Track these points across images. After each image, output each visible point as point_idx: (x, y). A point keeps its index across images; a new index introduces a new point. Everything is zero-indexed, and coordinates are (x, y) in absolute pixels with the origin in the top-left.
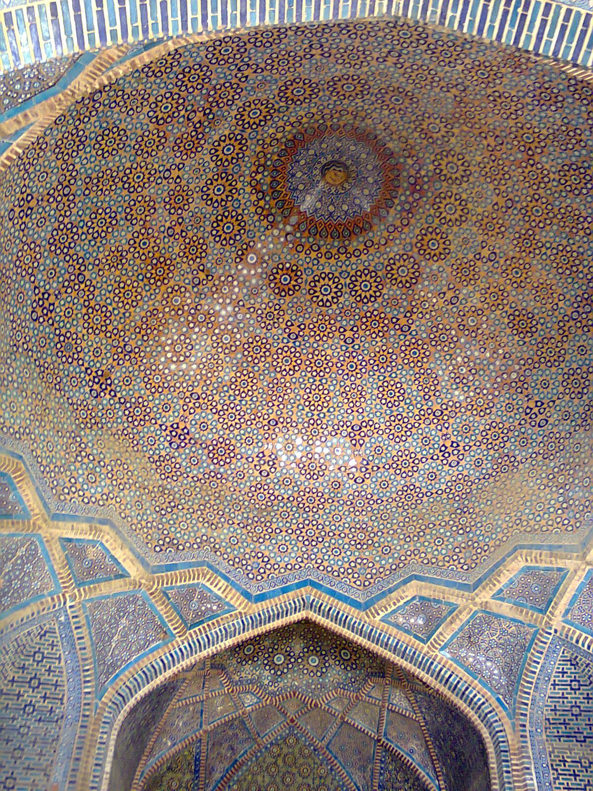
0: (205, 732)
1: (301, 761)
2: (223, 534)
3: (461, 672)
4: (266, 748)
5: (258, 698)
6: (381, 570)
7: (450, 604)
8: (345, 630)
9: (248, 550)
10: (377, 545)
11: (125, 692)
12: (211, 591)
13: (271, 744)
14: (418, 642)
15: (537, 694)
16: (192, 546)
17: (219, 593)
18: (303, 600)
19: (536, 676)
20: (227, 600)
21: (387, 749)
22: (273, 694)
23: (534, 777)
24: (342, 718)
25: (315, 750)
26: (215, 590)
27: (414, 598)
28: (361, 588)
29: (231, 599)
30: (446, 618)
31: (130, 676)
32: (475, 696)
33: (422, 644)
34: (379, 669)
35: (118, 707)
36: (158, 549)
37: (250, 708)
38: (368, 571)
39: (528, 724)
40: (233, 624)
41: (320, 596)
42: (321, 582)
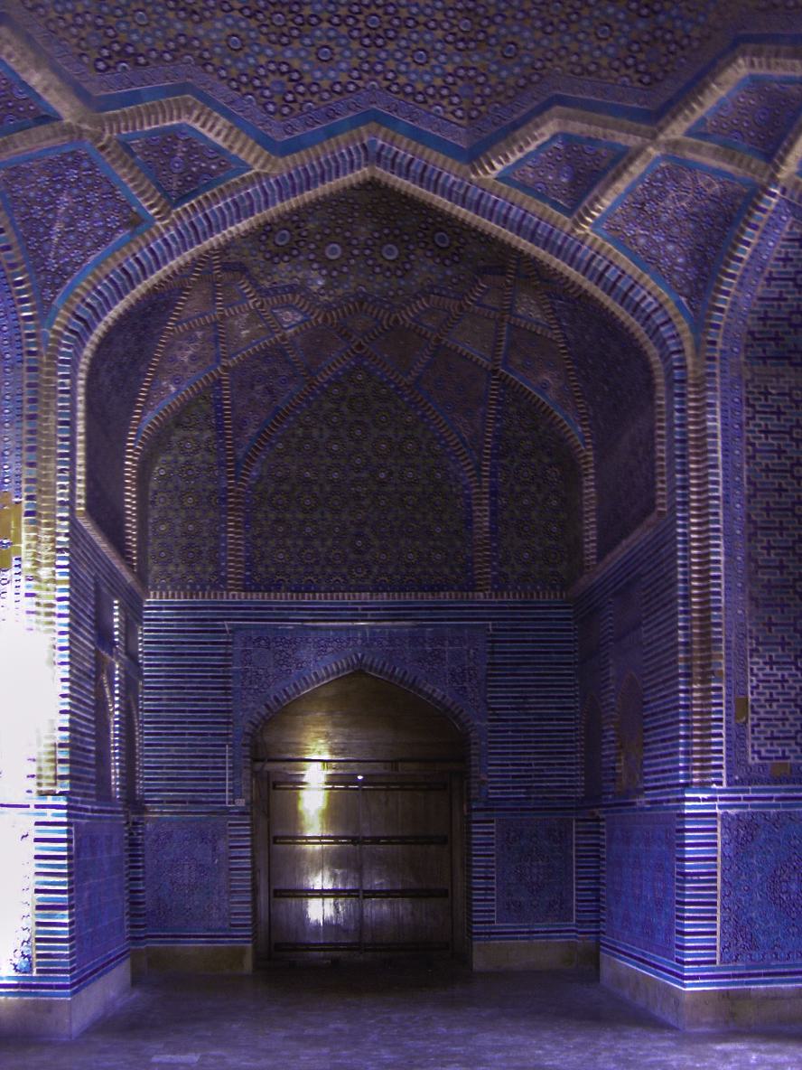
0: (225, 368)
2: (215, 30)
3: (624, 261)
4: (321, 388)
5: (304, 314)
6: (500, 88)
7: (612, 146)
8: (438, 197)
9: (263, 61)
10: (493, 41)
11: (86, 313)
13: (329, 382)
14: (557, 213)
16: (161, 56)
20: (234, 152)
22: (328, 306)
24: (438, 340)
25: (397, 388)
26: (211, 136)
27: (554, 137)
28: (463, 122)
29: (241, 150)
30: (605, 171)
31: (89, 287)
34: (500, 263)
35: (80, 338)
36: (101, 65)
37: (290, 331)
38: (477, 90)
42: (395, 115)
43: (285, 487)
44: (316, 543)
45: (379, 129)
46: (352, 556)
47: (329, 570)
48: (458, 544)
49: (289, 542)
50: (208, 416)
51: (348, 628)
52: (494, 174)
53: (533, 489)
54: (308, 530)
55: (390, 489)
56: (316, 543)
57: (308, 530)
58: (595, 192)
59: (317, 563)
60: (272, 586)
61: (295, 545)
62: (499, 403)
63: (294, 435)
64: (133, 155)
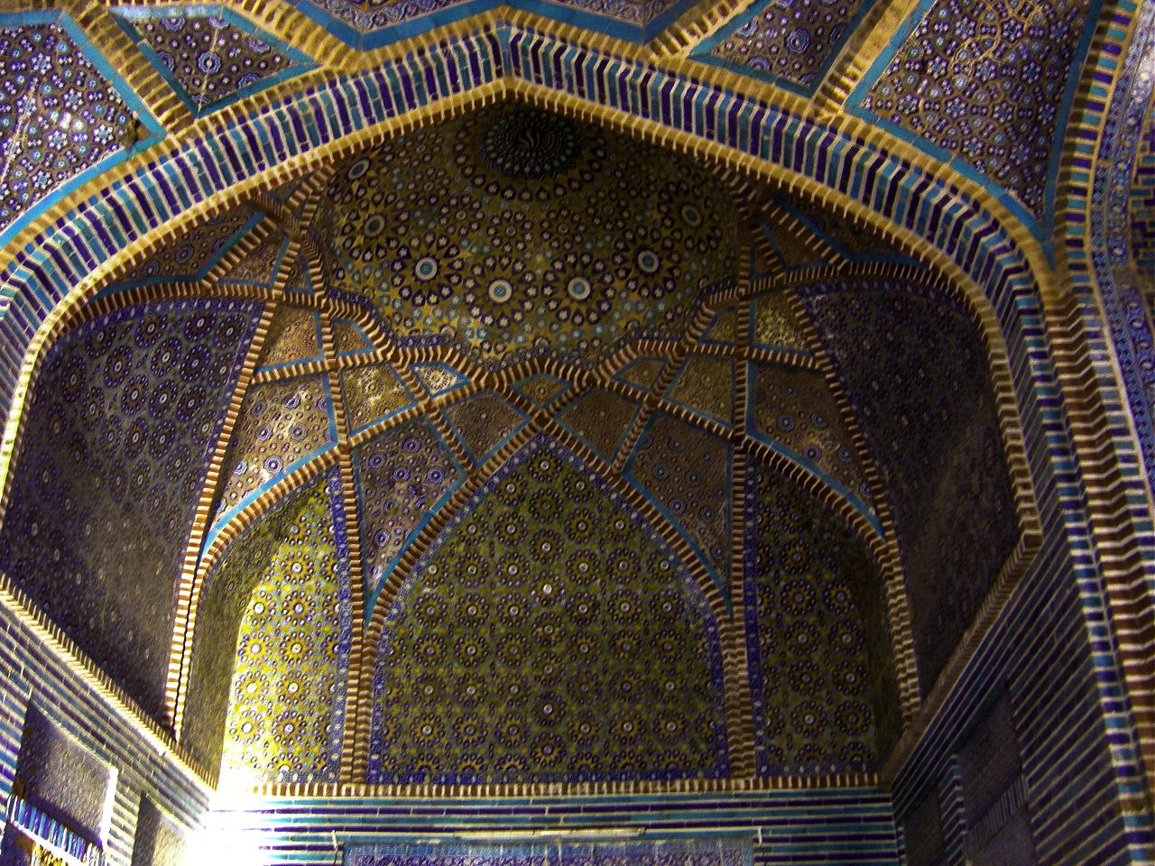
0: (346, 449)
1: (572, 506)
4: (490, 484)
8: (607, 108)
12: (253, 26)
13: (500, 474)
15: (1108, 165)
17: (271, 28)
18: (491, 38)
19: (1103, 115)
20: (294, 42)
21: (755, 459)
22: (495, 366)
23: (1111, 350)
24: (652, 403)
25: (599, 481)
26: (260, 21)
30: (857, 18)
32: (946, 199)
33: (799, 99)
37: (443, 397)
39: (1087, 240)
40: (314, 101)
41: (533, 22)
43: (438, 630)
44: (482, 710)
45: (511, 14)
46: (536, 729)
47: (500, 751)
48: (702, 707)
49: (440, 710)
50: (323, 523)
51: (528, 843)
52: (685, 52)
53: (812, 619)
54: (471, 690)
55: (595, 628)
56: (482, 710)
57: (471, 690)
58: (845, 50)
59: (482, 740)
60: (409, 775)
61: (449, 715)
62: (748, 489)
63: (452, 554)
64: (137, 38)
